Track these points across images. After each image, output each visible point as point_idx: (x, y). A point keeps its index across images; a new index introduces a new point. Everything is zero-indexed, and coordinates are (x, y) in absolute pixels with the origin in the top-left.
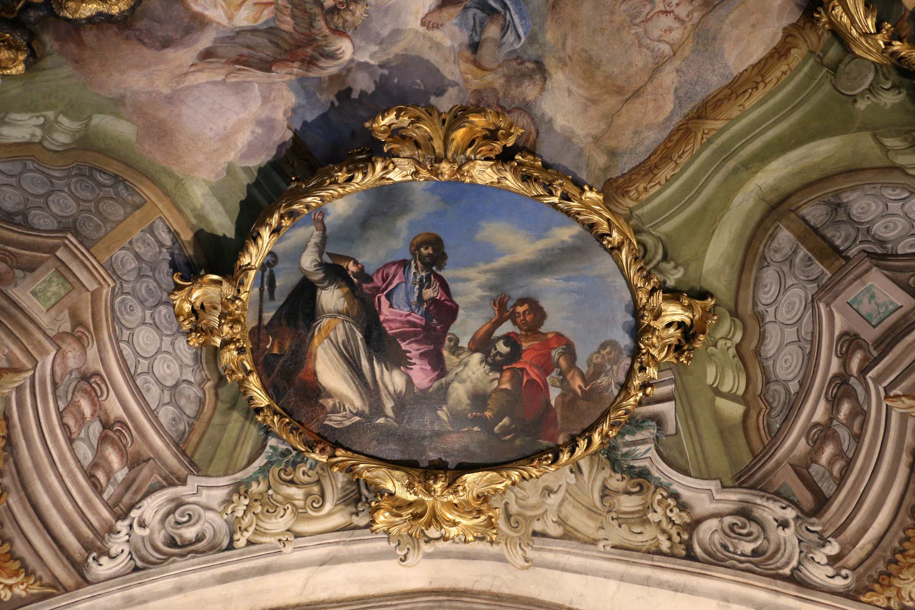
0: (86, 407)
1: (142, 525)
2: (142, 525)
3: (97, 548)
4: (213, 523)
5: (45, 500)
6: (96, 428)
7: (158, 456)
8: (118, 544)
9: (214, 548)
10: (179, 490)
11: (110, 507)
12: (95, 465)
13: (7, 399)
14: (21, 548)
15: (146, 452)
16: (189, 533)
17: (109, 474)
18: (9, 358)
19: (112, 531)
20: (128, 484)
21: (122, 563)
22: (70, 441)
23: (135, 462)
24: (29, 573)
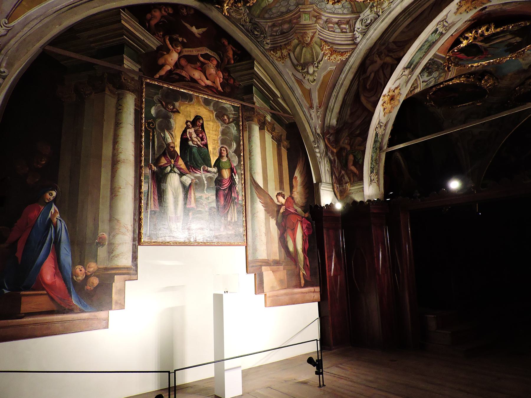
0: (331, 25)
1: (359, 29)
2: (359, 29)
3: (354, 38)
4: (372, 16)
5: (339, 42)
6: (336, 26)
7: (351, 18)
8: (357, 34)
9: (376, 19)
10: (360, 18)
11: (351, 32)
12: (342, 30)
13: (319, 37)
14: (342, 51)
15: (348, 20)
16: (369, 21)
17: (345, 29)
18: (312, 32)
19: (354, 35)
20: (350, 27)
21: (361, 36)
22: (334, 32)
23: (348, 23)
24: (347, 52)
